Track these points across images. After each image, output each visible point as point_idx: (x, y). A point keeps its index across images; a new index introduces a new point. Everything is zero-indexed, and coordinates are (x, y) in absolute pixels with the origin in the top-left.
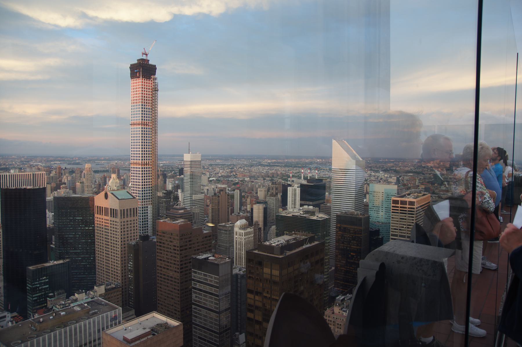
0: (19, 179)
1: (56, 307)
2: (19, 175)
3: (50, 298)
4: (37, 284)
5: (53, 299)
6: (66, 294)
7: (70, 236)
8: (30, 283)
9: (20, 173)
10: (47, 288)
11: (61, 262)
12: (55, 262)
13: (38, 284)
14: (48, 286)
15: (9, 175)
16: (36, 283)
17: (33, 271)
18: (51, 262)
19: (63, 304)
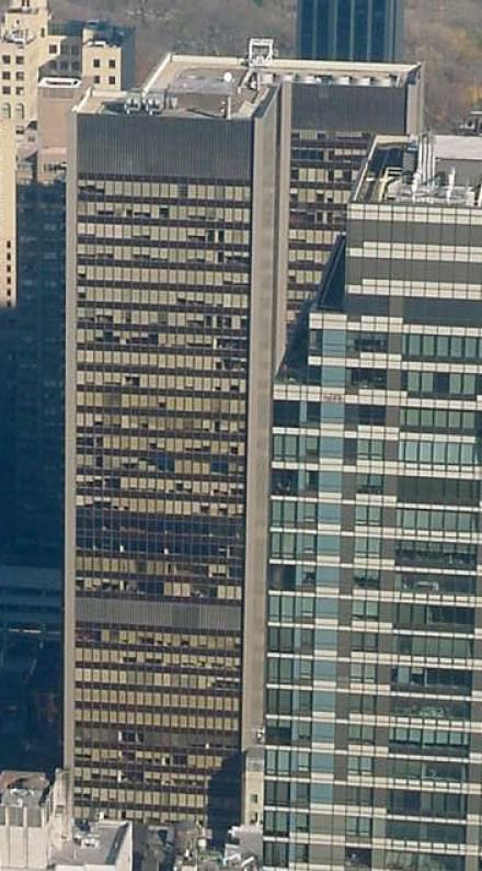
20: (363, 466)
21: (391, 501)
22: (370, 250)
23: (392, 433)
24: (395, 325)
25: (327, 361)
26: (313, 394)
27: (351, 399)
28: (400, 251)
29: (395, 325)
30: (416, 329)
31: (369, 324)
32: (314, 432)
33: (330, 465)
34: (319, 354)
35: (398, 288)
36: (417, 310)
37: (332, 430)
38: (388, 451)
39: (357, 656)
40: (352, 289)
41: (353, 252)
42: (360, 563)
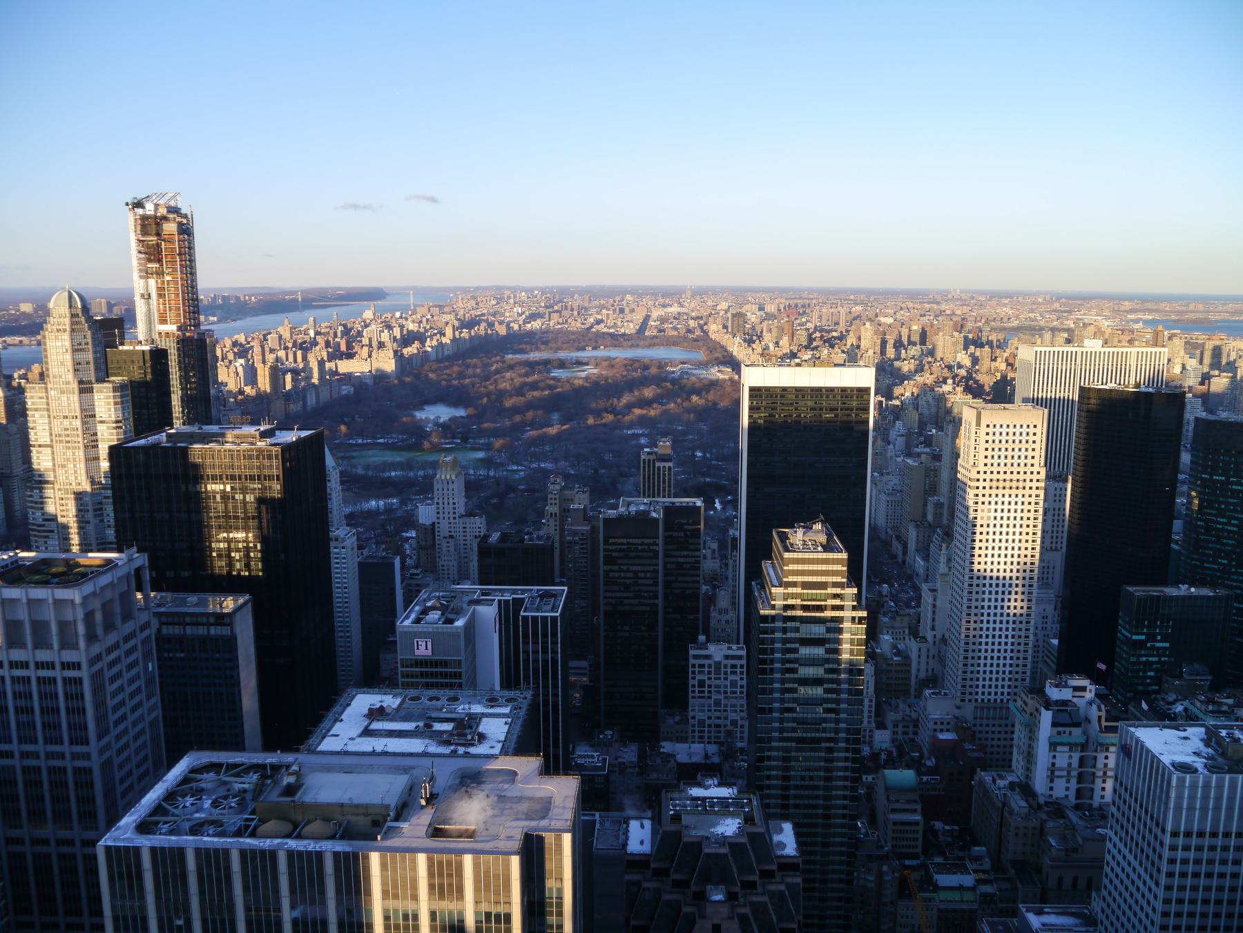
7: (1229, 528)
9: (1107, 350)
10: (1165, 648)
11: (1206, 592)
12: (1193, 590)
14: (1167, 645)
17: (1139, 599)
18: (1184, 587)
20: (789, 635)
22: (791, 567)
23: (798, 624)
24: (798, 590)
27: (785, 614)
28: (800, 567)
29: (798, 590)
30: (805, 591)
35: (799, 579)
36: (805, 585)
38: (797, 630)
39: (787, 695)
40: (785, 580)
41: (785, 568)
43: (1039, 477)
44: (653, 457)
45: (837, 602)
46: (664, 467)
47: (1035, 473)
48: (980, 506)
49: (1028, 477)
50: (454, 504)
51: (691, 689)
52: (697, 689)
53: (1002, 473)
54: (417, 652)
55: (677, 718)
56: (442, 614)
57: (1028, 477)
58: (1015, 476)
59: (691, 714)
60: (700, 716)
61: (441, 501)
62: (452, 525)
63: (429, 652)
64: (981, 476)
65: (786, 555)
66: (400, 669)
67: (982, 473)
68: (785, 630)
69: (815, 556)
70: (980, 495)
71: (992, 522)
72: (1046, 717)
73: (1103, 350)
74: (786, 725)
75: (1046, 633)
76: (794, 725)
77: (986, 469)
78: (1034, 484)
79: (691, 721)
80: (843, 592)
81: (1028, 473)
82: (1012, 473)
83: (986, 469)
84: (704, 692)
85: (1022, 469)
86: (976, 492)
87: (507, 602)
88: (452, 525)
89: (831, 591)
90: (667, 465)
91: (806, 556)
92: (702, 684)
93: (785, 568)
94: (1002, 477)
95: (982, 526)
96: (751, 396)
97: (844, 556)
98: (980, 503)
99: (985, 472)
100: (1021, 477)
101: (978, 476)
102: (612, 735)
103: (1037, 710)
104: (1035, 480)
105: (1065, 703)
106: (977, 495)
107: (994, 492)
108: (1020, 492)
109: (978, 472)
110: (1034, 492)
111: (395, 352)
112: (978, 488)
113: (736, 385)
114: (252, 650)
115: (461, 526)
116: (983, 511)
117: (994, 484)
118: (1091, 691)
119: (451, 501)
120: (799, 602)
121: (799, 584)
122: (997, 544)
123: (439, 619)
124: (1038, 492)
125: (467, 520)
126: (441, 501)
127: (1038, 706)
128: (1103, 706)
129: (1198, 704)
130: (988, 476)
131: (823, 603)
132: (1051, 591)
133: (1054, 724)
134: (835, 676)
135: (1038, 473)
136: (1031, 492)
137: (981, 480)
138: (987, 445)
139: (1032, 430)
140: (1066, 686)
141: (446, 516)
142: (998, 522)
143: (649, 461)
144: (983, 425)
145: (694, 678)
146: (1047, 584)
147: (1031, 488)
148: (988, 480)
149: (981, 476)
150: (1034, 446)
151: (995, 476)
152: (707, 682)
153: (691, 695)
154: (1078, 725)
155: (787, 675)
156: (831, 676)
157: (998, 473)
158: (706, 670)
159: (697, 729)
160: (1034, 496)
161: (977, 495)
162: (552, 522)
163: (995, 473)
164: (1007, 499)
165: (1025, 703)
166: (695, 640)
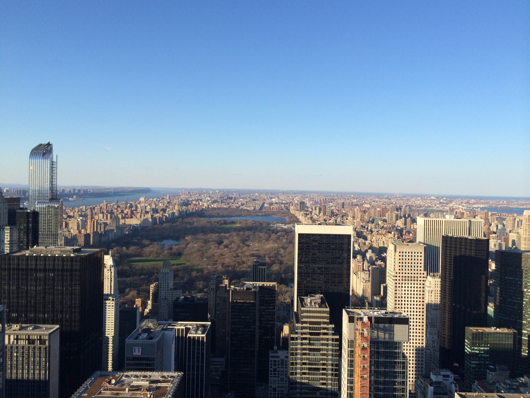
0: (455, 226)
1: (500, 384)
2: (455, 221)
3: (491, 371)
4: (476, 350)
5: (493, 373)
6: (509, 372)
8: (469, 346)
9: (456, 220)
12: (498, 329)
13: (478, 350)
15: (445, 221)
16: (475, 348)
19: (509, 385)
20: (304, 347)
21: (308, 352)
22: (304, 314)
23: (308, 341)
24: (308, 325)
25: (299, 331)
26: (296, 336)
27: (302, 336)
28: (308, 314)
29: (308, 325)
30: (311, 326)
31: (304, 325)
32: (296, 342)
33: (299, 346)
34: (297, 330)
35: (308, 320)
36: (311, 323)
37: (299, 341)
41: (302, 315)
42: (303, 361)
43: (424, 276)
44: (258, 264)
45: (325, 331)
46: (262, 268)
47: (422, 274)
48: (398, 288)
49: (419, 275)
50: (168, 283)
51: (270, 373)
52: (273, 373)
53: (407, 273)
54: (134, 354)
55: (264, 387)
56: (148, 335)
57: (419, 275)
58: (413, 275)
59: (270, 385)
60: (274, 386)
61: (162, 282)
62: (166, 293)
63: (140, 354)
64: (398, 275)
65: (302, 309)
66: (126, 362)
67: (398, 273)
68: (302, 344)
69: (315, 309)
70: (398, 283)
71: (403, 296)
72: (431, 389)
73: (454, 220)
74: (303, 391)
75: (434, 349)
76: (307, 391)
77: (400, 271)
78: (422, 279)
79: (270, 389)
80: (328, 326)
81: (419, 274)
82: (411, 273)
83: (400, 271)
84: (275, 374)
85: (416, 272)
86: (396, 282)
87: (182, 330)
88: (166, 293)
89: (322, 326)
90: (263, 267)
91: (311, 309)
92: (275, 370)
93: (302, 315)
94: (407, 275)
95: (399, 297)
96: (299, 238)
97: (328, 309)
98: (398, 287)
99: (399, 273)
100: (416, 275)
101: (396, 275)
102: (231, 395)
103: (427, 386)
104: (422, 277)
105: (439, 383)
106: (396, 283)
107: (404, 282)
108: (416, 282)
109: (396, 273)
110: (422, 282)
111: (152, 216)
112: (396, 280)
113: (290, 232)
114: (58, 353)
115: (171, 294)
116: (399, 290)
117: (404, 278)
118: (451, 378)
119: (167, 282)
120: (308, 331)
121: (308, 323)
122: (406, 306)
123: (146, 337)
124: (424, 282)
125: (174, 291)
126: (162, 282)
127: (427, 384)
128: (457, 385)
129: (503, 385)
130: (401, 275)
131: (319, 331)
132: (435, 329)
133: (435, 393)
134: (325, 367)
135: (423, 274)
136: (420, 282)
137: (398, 276)
138: (400, 261)
139: (419, 255)
140: (440, 375)
141: (164, 289)
142: (406, 296)
143: (256, 265)
144: (398, 251)
145: (271, 367)
146: (434, 325)
147: (420, 281)
148: (401, 277)
149: (398, 275)
150: (421, 262)
151: (404, 275)
152: (277, 369)
153: (270, 375)
154: (445, 394)
155: (303, 366)
156: (323, 367)
157: (405, 273)
158: (277, 363)
159: (272, 393)
160: (422, 284)
161: (396, 283)
162: (212, 293)
163: (404, 273)
164: (410, 285)
165: (421, 383)
166: (272, 348)
